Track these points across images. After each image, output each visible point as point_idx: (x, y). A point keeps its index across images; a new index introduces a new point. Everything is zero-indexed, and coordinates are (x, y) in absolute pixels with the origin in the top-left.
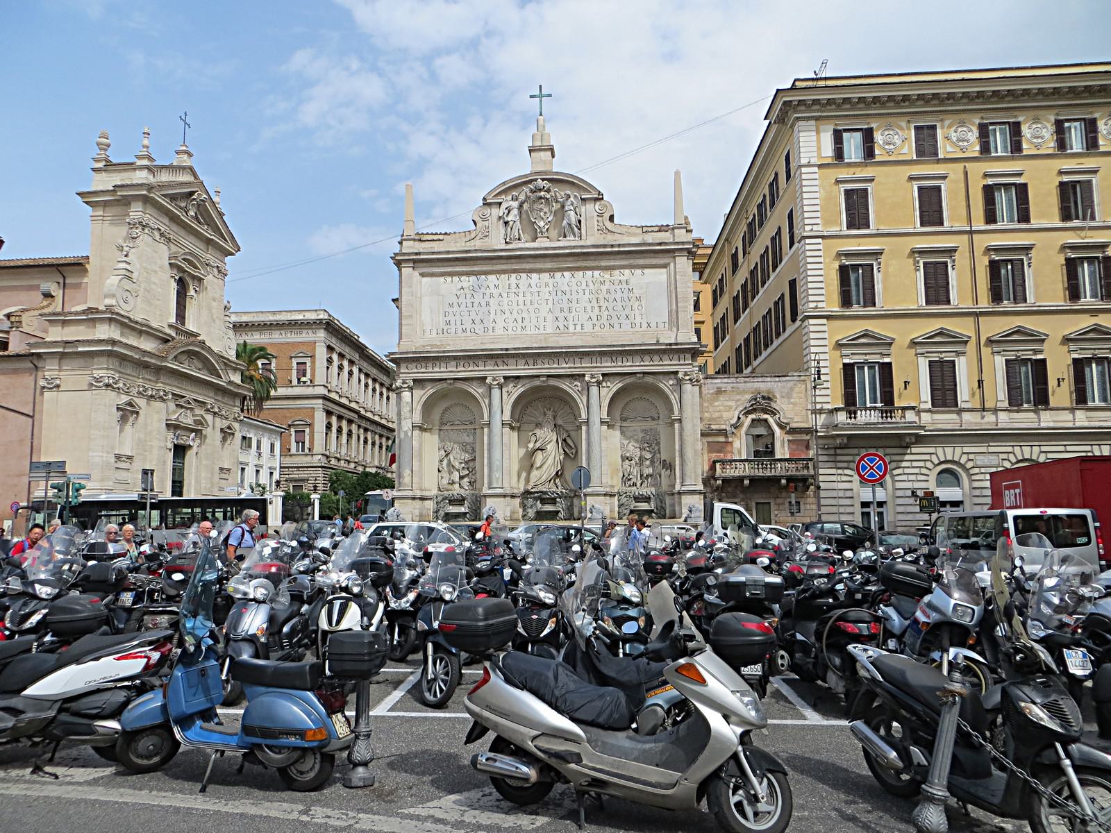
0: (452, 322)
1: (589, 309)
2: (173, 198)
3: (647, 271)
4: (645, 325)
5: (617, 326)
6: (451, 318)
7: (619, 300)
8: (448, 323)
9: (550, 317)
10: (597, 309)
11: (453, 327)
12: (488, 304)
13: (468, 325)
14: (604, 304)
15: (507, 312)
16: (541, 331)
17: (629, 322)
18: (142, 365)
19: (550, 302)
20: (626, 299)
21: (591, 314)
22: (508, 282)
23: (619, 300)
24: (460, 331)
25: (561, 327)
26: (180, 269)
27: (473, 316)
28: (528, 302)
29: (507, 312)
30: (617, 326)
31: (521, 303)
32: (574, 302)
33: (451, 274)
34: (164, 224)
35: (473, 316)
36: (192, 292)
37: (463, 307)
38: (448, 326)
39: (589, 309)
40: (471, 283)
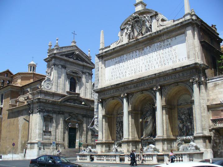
0: (114, 76)
1: (156, 59)
2: (67, 55)
3: (177, 37)
4: (178, 61)
5: (167, 64)
6: (113, 74)
7: (167, 52)
8: (112, 76)
9: (144, 66)
10: (159, 58)
11: (114, 77)
12: (124, 66)
13: (118, 75)
14: (161, 56)
15: (130, 67)
16: (141, 72)
17: (171, 61)
18: (54, 103)
19: (143, 60)
20: (170, 51)
21: (157, 61)
22: (129, 56)
23: (167, 52)
24: (116, 78)
25: (147, 69)
26: (70, 75)
27: (120, 71)
28: (136, 62)
29: (130, 67)
30: (167, 64)
31: (134, 63)
32: (151, 57)
33: (113, 58)
34: (62, 63)
35: (120, 71)
36: (77, 81)
37: (117, 69)
38: (113, 77)
39: (156, 59)
40: (119, 59)
